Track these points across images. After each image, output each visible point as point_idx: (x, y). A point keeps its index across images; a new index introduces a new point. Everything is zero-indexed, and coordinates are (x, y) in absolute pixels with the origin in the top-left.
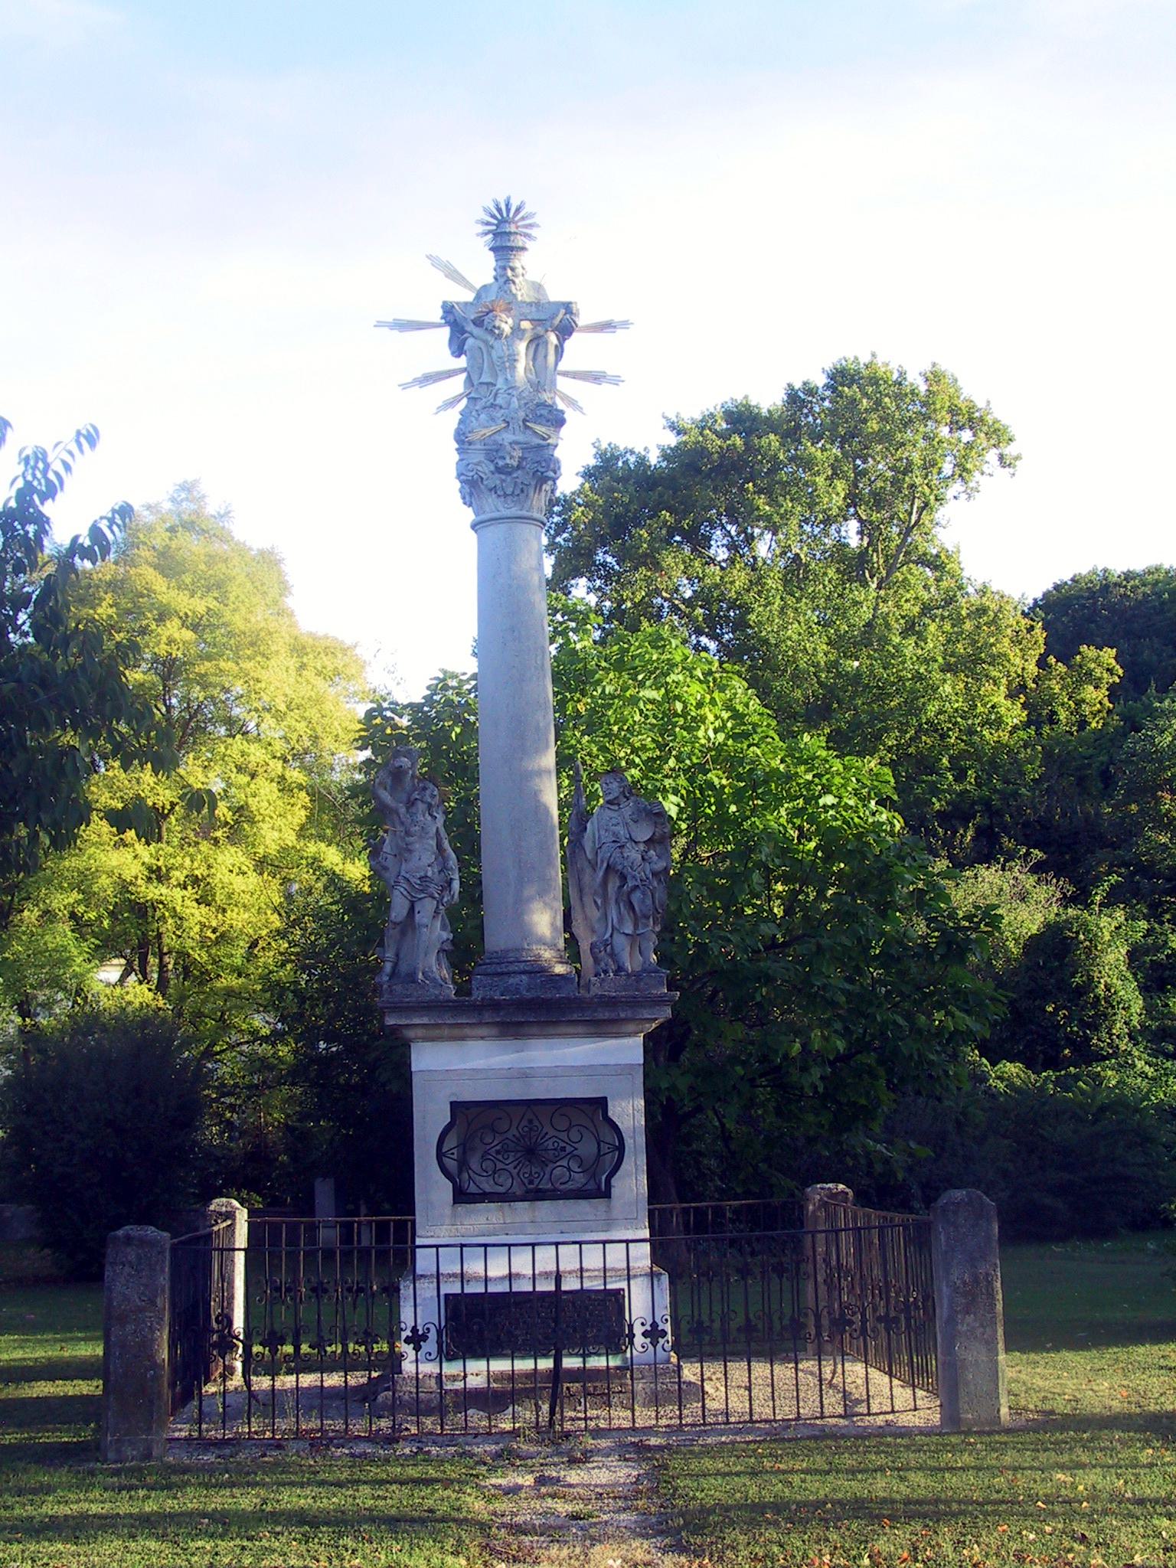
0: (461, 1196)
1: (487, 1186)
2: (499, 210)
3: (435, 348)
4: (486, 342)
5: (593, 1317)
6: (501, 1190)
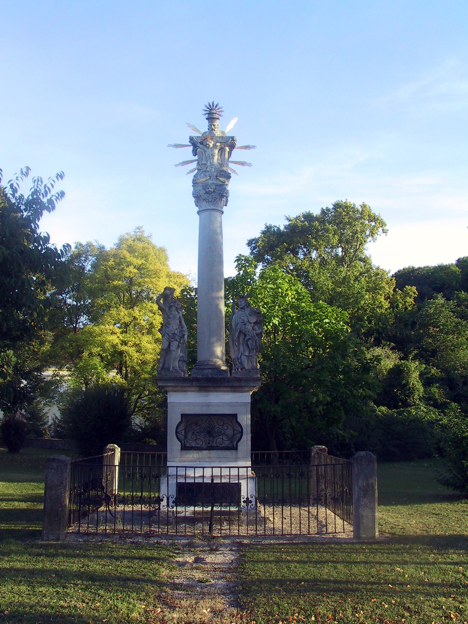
0: (185, 448)
1: (194, 444)
2: (210, 106)
3: (188, 153)
4: (204, 150)
5: (228, 492)
6: (199, 446)
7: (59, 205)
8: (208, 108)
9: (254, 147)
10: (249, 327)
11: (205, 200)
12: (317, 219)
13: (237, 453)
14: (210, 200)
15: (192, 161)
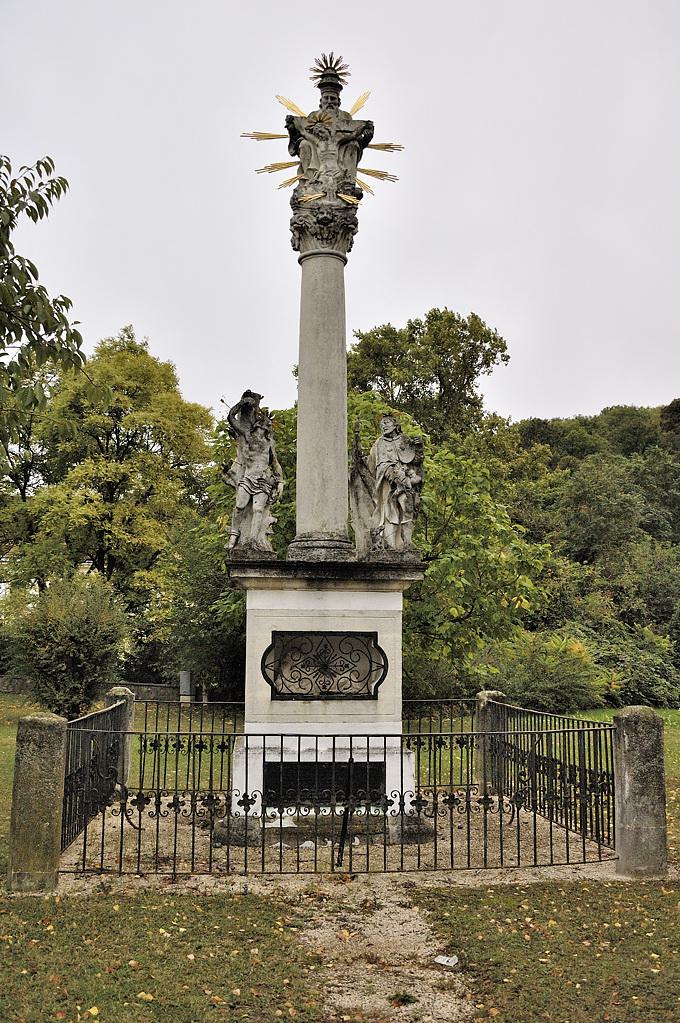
0: (277, 695)
1: (295, 688)
2: (325, 61)
3: (280, 150)
4: (313, 143)
5: (365, 779)
6: (304, 692)
7: (55, 206)
8: (321, 66)
9: (399, 148)
10: (400, 471)
11: (315, 234)
12: (400, 335)
13: (376, 705)
14: (325, 236)
15: (289, 165)
